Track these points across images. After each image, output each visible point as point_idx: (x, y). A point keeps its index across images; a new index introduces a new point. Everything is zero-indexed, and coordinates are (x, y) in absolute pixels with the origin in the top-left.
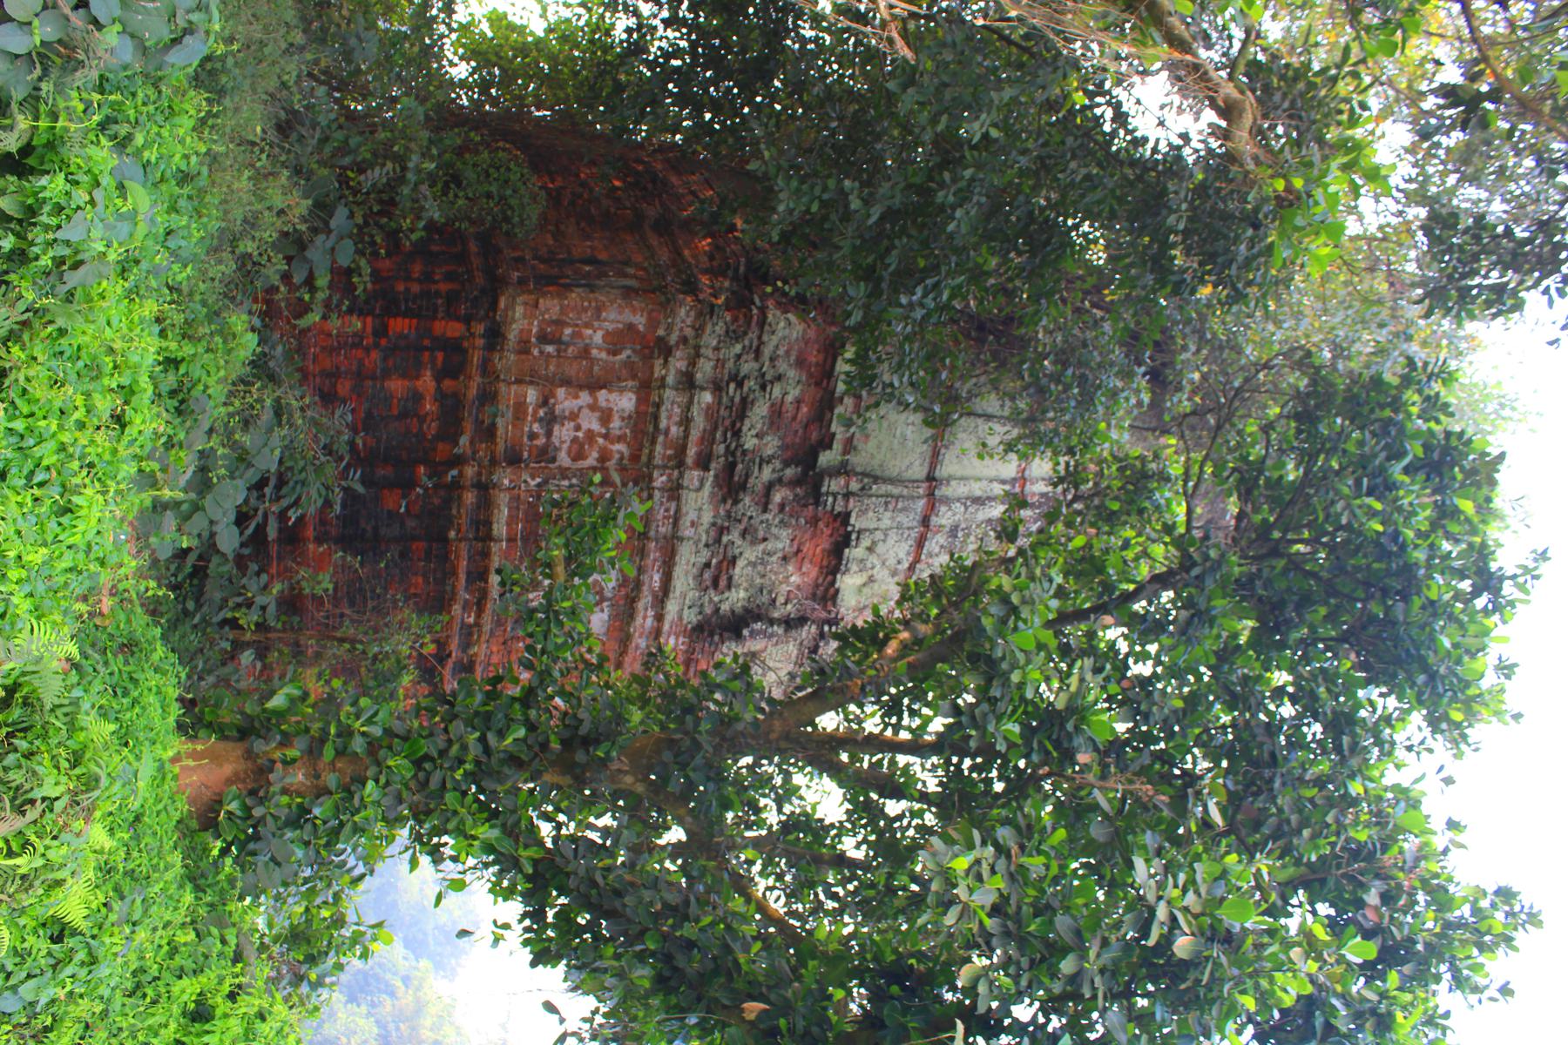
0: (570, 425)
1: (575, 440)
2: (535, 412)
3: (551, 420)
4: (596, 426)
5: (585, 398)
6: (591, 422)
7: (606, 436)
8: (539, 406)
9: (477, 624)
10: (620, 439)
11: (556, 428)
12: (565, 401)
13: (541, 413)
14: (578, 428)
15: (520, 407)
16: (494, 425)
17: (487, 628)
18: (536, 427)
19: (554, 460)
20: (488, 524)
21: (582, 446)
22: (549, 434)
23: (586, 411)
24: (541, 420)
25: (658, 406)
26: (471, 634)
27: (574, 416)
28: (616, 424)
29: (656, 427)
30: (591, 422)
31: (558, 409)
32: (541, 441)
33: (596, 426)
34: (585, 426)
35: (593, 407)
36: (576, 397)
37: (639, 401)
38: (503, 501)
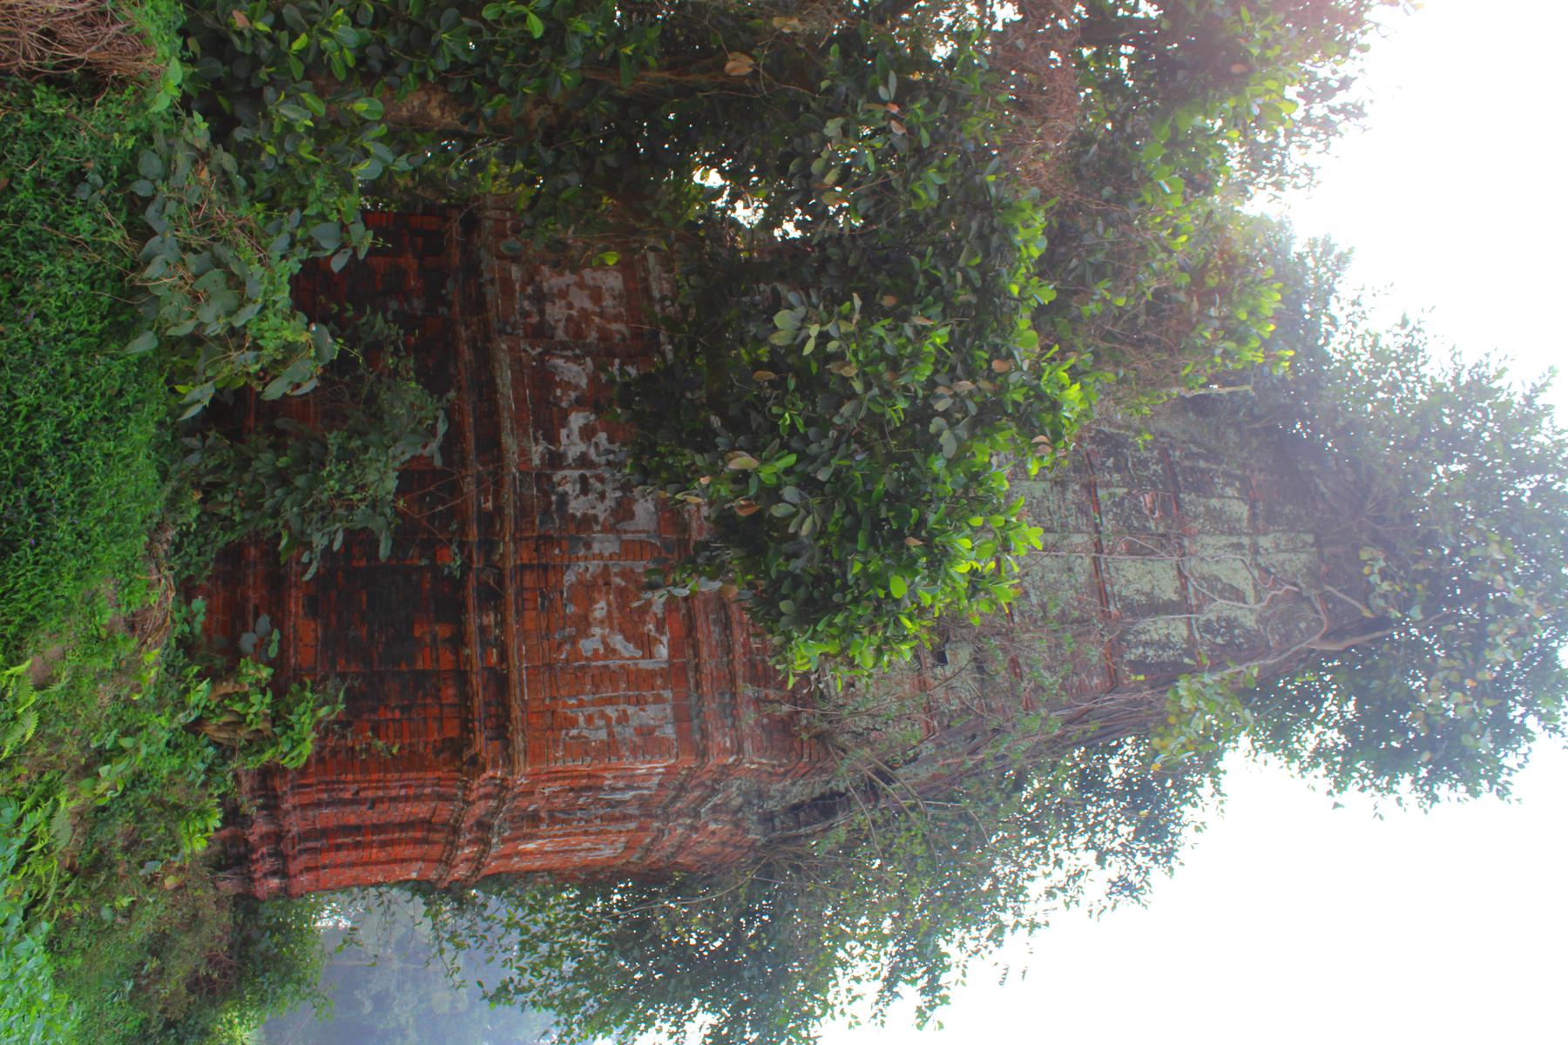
0: (561, 303)
1: (569, 319)
2: (523, 290)
3: (540, 298)
4: (588, 305)
5: (569, 278)
6: (582, 301)
7: (601, 315)
8: (524, 285)
9: (499, 510)
10: (617, 318)
11: (549, 308)
12: (552, 281)
13: (529, 290)
14: (570, 306)
15: (507, 283)
16: (482, 295)
17: (510, 511)
18: (526, 303)
19: (552, 337)
20: (492, 381)
21: (578, 325)
22: (542, 312)
23: (574, 290)
24: (529, 297)
25: (646, 279)
26: (492, 525)
27: (563, 294)
28: (608, 302)
29: (650, 298)
30: (582, 301)
31: (545, 286)
32: (535, 319)
33: (588, 305)
34: (577, 304)
35: (581, 285)
36: (561, 274)
37: (625, 281)
38: (504, 378)
